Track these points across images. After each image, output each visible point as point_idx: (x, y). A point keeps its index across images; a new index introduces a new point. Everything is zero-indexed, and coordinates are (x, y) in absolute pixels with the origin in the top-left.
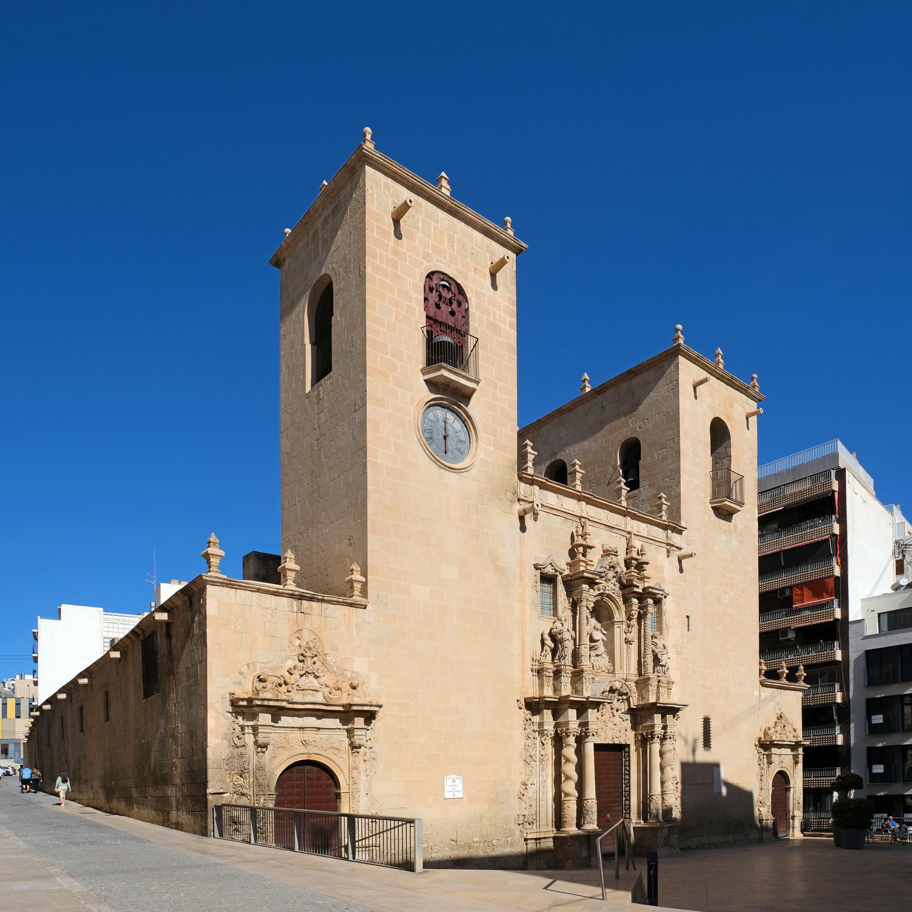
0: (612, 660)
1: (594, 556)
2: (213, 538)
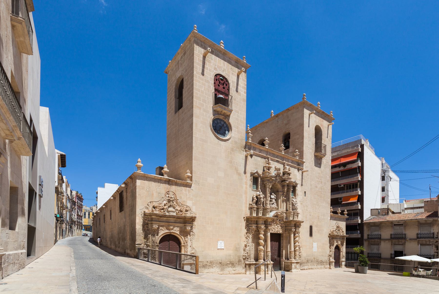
0: (278, 205)
2: (139, 160)
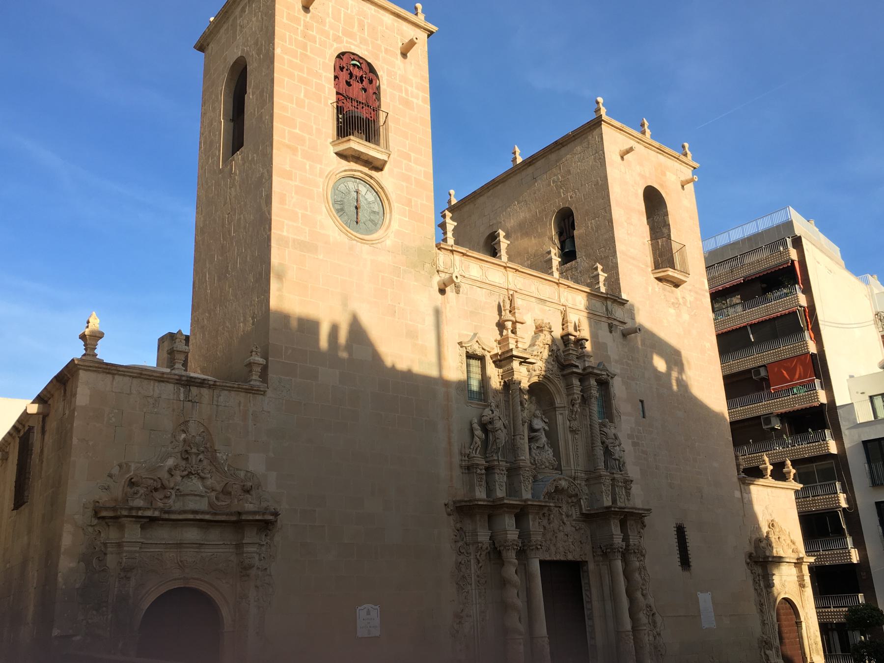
1: (526, 333)
